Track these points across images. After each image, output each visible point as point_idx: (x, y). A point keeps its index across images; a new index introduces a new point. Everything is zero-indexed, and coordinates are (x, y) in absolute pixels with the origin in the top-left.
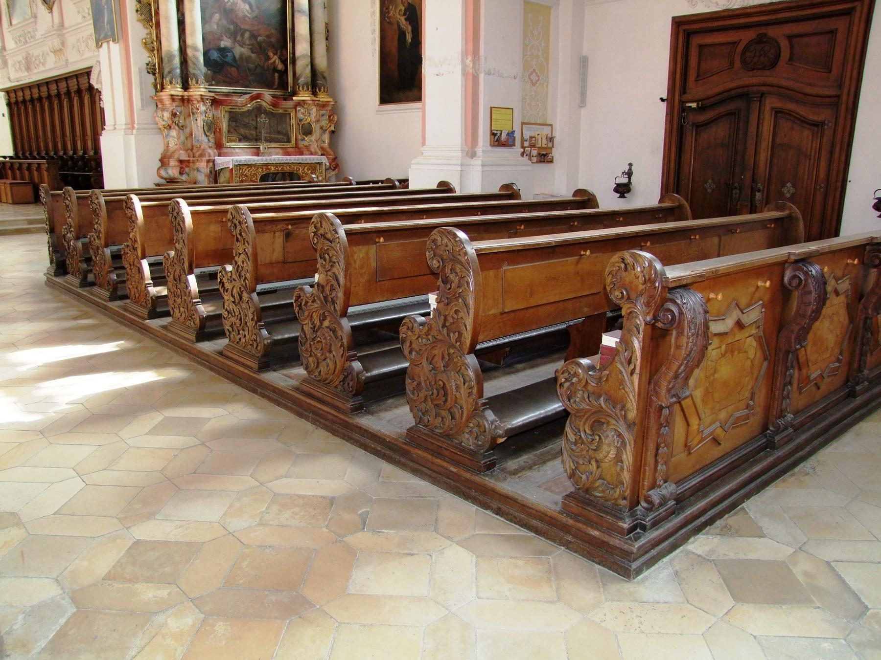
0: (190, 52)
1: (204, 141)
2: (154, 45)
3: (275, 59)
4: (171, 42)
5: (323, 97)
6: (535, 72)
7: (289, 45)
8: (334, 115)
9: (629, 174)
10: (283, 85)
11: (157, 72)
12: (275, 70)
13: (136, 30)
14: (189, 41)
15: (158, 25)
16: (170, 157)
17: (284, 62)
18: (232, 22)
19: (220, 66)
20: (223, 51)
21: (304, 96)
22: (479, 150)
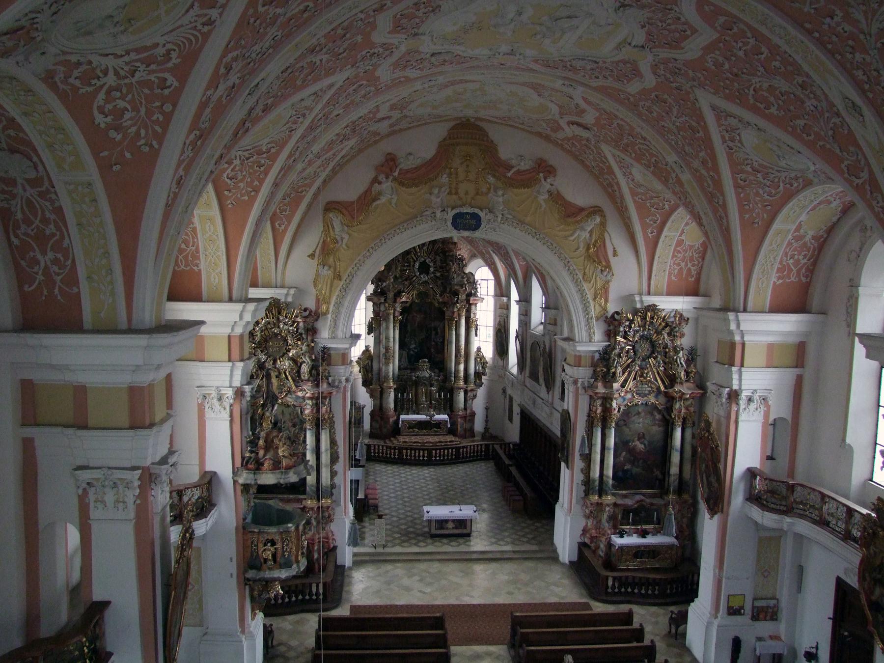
2: (587, 471)
3: (657, 473)
4: (596, 473)
5: (686, 496)
11: (587, 482)
14: (605, 472)
17: (663, 474)
19: (622, 479)
20: (625, 472)
22: (719, 615)
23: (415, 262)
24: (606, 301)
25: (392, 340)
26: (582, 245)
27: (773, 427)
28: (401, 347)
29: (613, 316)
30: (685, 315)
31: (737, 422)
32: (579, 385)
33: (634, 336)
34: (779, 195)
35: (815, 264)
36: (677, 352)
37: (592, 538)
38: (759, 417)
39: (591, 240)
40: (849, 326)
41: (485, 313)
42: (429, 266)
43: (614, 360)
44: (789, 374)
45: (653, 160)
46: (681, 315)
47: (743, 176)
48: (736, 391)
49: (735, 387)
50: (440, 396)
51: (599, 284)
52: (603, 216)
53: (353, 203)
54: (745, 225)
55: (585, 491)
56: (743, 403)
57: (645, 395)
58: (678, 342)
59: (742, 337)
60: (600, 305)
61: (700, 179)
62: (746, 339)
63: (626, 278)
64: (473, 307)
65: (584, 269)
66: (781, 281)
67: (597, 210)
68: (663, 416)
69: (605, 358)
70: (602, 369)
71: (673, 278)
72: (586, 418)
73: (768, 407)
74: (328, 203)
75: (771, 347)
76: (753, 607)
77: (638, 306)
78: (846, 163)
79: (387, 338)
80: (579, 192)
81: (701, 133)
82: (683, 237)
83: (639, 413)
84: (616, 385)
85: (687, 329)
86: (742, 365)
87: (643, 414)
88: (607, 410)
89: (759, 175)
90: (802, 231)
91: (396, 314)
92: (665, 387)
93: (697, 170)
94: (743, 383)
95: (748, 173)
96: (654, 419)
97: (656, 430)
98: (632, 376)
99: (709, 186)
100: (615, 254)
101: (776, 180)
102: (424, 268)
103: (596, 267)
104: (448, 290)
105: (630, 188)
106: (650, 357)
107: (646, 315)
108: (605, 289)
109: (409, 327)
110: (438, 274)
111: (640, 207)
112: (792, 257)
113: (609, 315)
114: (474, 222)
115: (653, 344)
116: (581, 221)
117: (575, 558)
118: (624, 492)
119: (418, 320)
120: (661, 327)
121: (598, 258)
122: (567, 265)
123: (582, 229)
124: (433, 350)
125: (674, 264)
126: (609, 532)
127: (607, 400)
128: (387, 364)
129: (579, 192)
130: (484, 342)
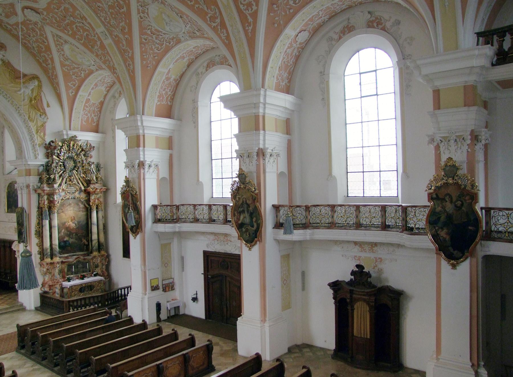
0: (54, 246)
1: (58, 276)
2: (41, 244)
3: (84, 241)
4: (47, 244)
5: (103, 252)
6: (166, 263)
7: (90, 235)
8: (108, 258)
9: (197, 294)
10: (87, 249)
12: (85, 245)
13: (34, 240)
14: (53, 243)
15: (42, 237)
16: (46, 283)
17: (88, 241)
18: (68, 231)
19: (64, 247)
20: (65, 242)
21: (95, 253)
22: (147, 293)
24: (45, 135)
26: (26, 98)
27: (161, 182)
29: (50, 144)
30: (93, 145)
31: (144, 179)
32: (31, 187)
33: (64, 156)
34: (162, 50)
35: (174, 95)
36: (90, 165)
37: (50, 286)
38: (154, 176)
39: (32, 95)
40: (194, 123)
43: (54, 170)
44: (167, 153)
45: (85, 34)
46: (90, 145)
47: (146, 37)
48: (142, 161)
49: (142, 159)
51: (40, 124)
52: (40, 81)
54: (144, 67)
55: (40, 258)
56: (147, 167)
57: (73, 193)
58: (89, 160)
59: (144, 131)
60: (41, 137)
61: (117, 42)
62: (146, 132)
63: (56, 122)
65: (29, 114)
66: (159, 103)
67: (35, 77)
68: (84, 205)
69: (47, 168)
70: (45, 176)
71: (84, 123)
72: (37, 209)
73: (158, 170)
75: (157, 138)
76: (163, 285)
77: (65, 137)
78: (209, 15)
80: (24, 64)
81: (125, 8)
82: (90, 98)
83: (70, 204)
84: (56, 186)
85: (93, 153)
86: (144, 147)
87: (73, 205)
88: (51, 202)
89: (154, 36)
90: (169, 75)
92: (84, 187)
93: (117, 36)
94: (146, 156)
95: (148, 35)
96: (80, 208)
97: (82, 215)
98: (65, 179)
99: (123, 45)
100: (48, 106)
101: (162, 40)
103: (36, 114)
105: (61, 61)
106: (74, 169)
107: (70, 143)
108: (43, 126)
111: (66, 76)
112: (164, 90)
113: (47, 143)
115: (75, 161)
117: (39, 304)
118: (66, 255)
120: (79, 151)
121: (37, 107)
122: (17, 109)
125: (84, 114)
126: (61, 280)
127: (51, 195)
129: (24, 64)
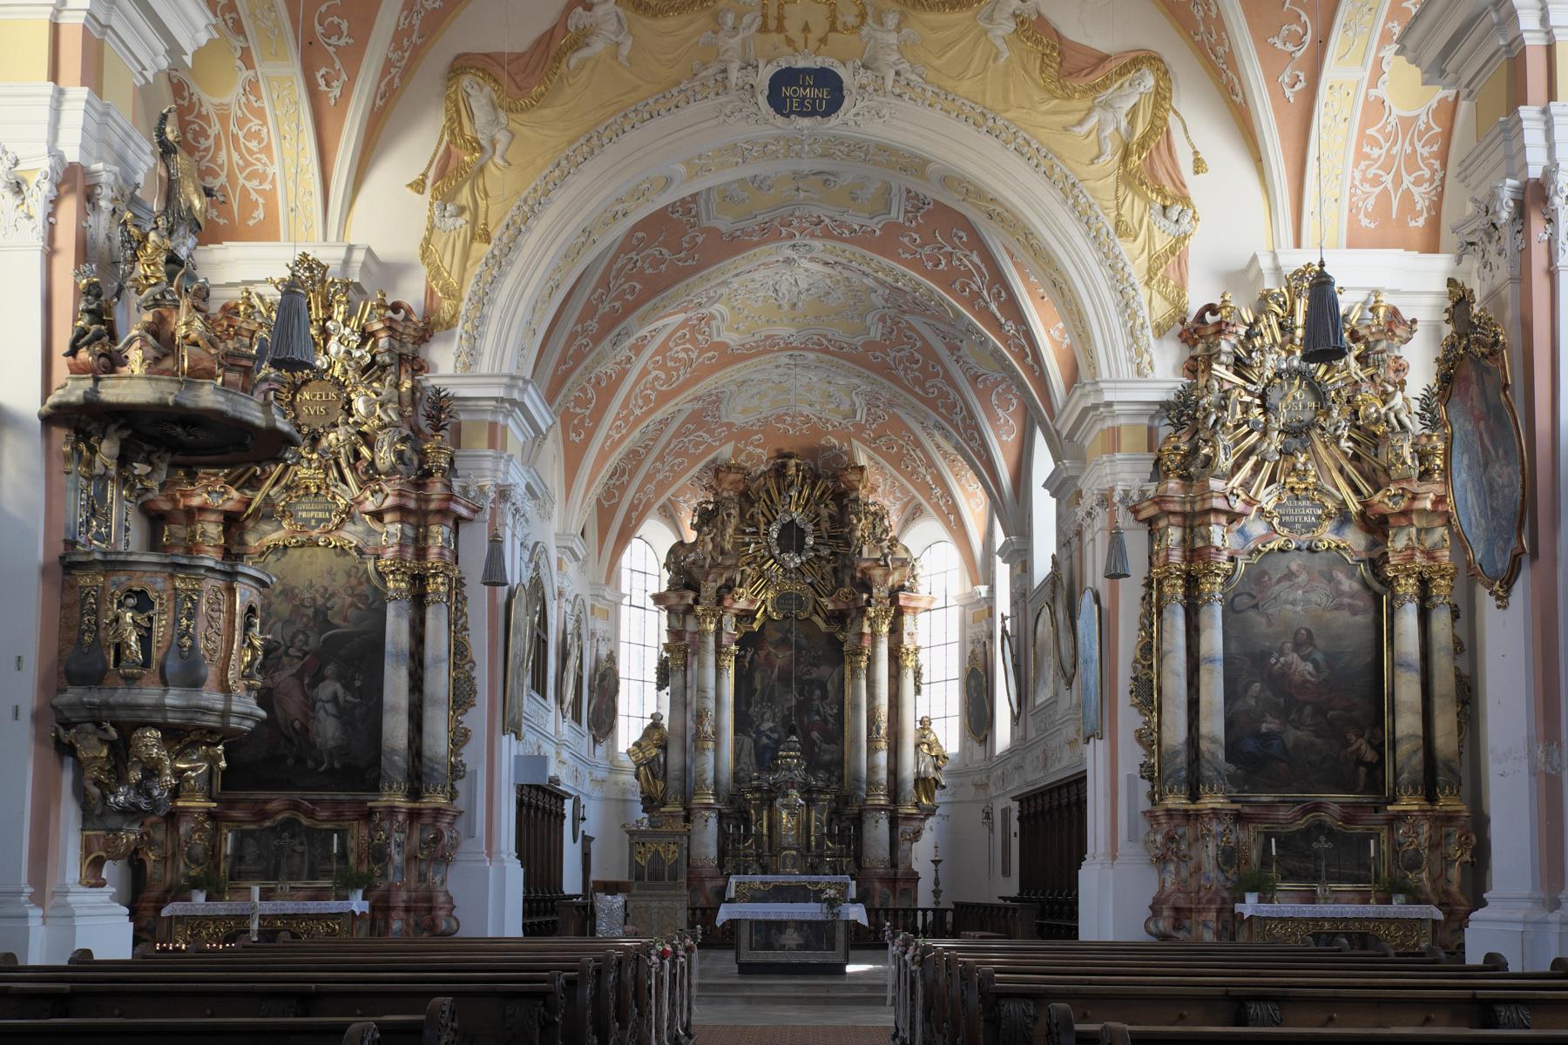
23: (769, 523)
25: (711, 693)
28: (742, 723)
41: (936, 640)
42: (802, 533)
50: (830, 829)
53: (519, 56)
64: (907, 619)
67: (1140, 60)
74: (458, 57)
79: (701, 690)
82: (1381, 91)
91: (725, 640)
102: (791, 537)
104: (847, 580)
109: (758, 676)
110: (825, 552)
114: (824, 94)
116: (1104, 85)
119: (779, 662)
123: (1107, 105)
124: (815, 735)
125: (1364, 180)
128: (701, 751)
130: (937, 708)
